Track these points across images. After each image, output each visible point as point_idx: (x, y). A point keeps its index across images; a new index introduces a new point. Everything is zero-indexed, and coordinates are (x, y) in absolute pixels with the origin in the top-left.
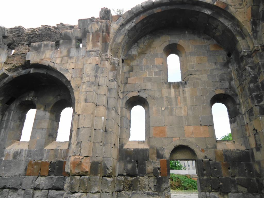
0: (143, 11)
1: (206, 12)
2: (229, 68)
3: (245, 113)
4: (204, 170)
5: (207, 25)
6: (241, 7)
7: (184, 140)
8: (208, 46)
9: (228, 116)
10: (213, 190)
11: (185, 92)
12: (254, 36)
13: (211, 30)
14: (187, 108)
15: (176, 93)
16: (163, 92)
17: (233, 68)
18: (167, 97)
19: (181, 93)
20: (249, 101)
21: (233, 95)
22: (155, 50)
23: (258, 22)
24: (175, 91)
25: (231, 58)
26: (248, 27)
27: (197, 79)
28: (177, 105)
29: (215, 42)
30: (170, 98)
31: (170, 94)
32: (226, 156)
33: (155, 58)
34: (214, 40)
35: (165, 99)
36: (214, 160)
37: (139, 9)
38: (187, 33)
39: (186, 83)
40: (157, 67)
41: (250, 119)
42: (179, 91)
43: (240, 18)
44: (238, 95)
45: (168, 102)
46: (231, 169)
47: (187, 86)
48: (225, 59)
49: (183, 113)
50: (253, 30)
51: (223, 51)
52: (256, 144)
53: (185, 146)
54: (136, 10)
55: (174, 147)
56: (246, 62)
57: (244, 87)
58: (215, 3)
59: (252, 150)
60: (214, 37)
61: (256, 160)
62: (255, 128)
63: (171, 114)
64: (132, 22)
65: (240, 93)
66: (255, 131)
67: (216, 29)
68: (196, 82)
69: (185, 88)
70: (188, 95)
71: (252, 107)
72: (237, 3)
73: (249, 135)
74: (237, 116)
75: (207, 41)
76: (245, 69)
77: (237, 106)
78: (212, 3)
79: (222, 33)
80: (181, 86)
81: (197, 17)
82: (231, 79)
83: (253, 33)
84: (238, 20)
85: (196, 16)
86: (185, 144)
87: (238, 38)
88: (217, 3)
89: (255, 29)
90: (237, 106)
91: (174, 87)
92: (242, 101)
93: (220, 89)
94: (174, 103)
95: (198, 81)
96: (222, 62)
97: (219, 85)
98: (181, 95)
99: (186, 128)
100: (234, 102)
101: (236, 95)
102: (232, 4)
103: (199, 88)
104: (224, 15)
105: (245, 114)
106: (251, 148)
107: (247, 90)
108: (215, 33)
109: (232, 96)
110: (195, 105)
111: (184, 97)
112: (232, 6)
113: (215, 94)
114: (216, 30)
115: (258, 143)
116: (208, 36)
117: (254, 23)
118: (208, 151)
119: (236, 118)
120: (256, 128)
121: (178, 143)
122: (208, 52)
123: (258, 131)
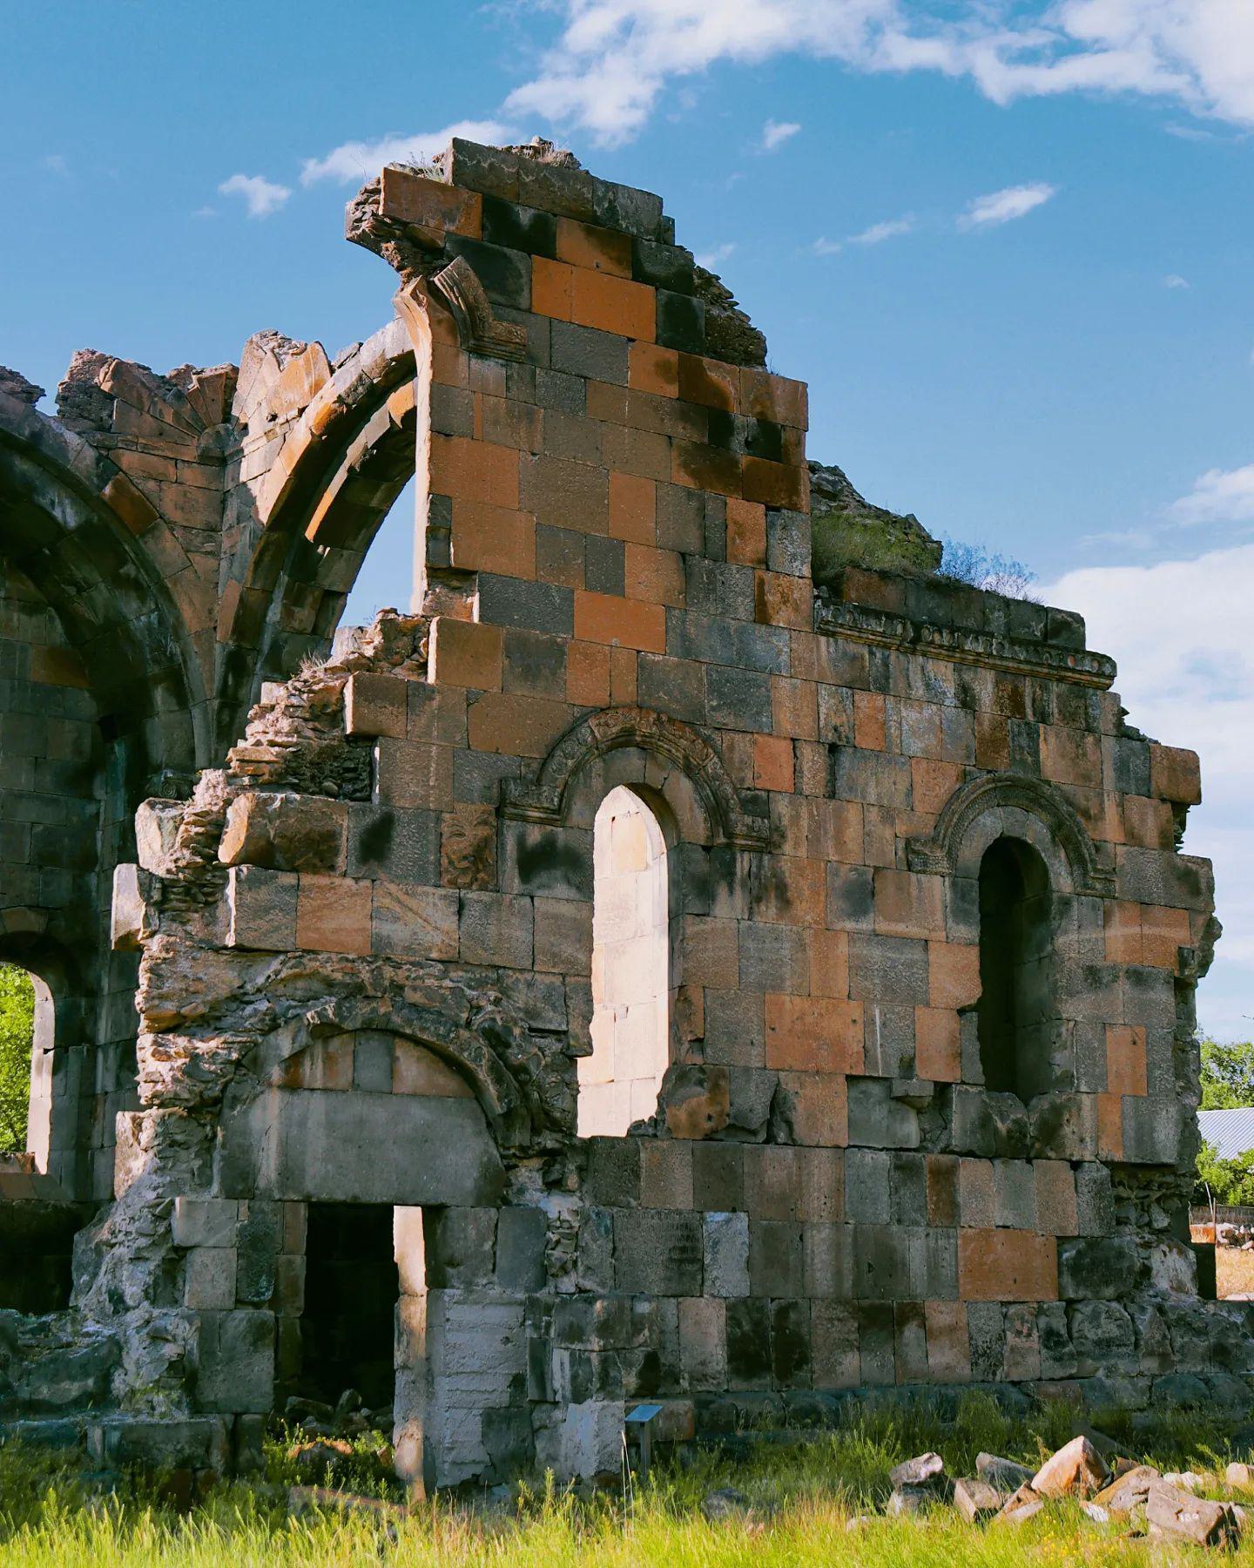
1: (57, 513)
2: (90, 798)
6: (209, 547)
12: (219, 722)
41: (118, 1078)
44: (101, 950)
50: (223, 691)
51: (87, 695)
72: (199, 520)
75: (24, 617)
88: (115, 487)
89: (230, 691)
93: (30, 907)
97: (27, 885)
102: (177, 516)
105: (105, 1047)
112: (172, 530)
116: (30, 587)
122: (12, 689)
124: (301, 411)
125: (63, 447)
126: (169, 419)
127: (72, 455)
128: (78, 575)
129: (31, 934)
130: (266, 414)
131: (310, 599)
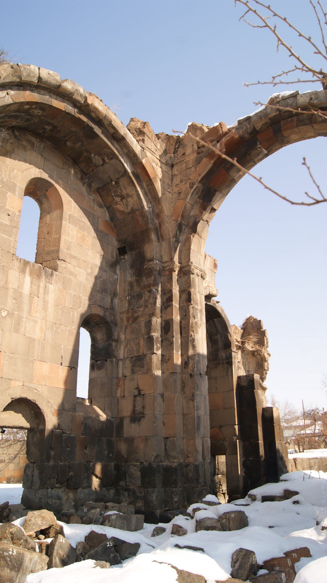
0: (35, 84)
2: (115, 272)
3: (124, 359)
4: (52, 449)
5: (114, 183)
6: (169, 190)
7: (30, 389)
8: (98, 218)
9: (90, 354)
10: (57, 486)
11: (48, 292)
13: (113, 194)
14: (46, 325)
15: (34, 287)
16: (9, 276)
17: (124, 276)
18: (15, 291)
19: (41, 291)
20: (142, 343)
21: (112, 322)
22: (12, 175)
23: (183, 228)
24: (32, 283)
25: (124, 259)
26: (169, 227)
27: (72, 273)
28: (29, 312)
29: (107, 217)
30: (21, 295)
31: (21, 285)
32: (85, 425)
33: (9, 193)
34: (107, 213)
35: (11, 293)
36: (68, 432)
37: (34, 77)
38: (72, 172)
39: (52, 274)
40: (9, 215)
42: (39, 286)
43: (167, 209)
45: (14, 301)
46: (88, 449)
47: (53, 282)
48: (115, 256)
49: (37, 335)
50: (176, 236)
52: (134, 411)
53: (30, 400)
54: (28, 75)
55: (10, 401)
56: (154, 281)
57: (138, 317)
58: (144, 161)
59: (122, 420)
60: (109, 208)
61: (125, 435)
62: (139, 387)
63: (17, 331)
64: (8, 94)
65: (125, 323)
66: (136, 392)
67: (122, 198)
68: (69, 279)
69: (49, 282)
70: (51, 298)
71: (145, 353)
73: (122, 396)
74: (108, 360)
75: (98, 208)
76: (150, 291)
77: (114, 344)
78: (140, 157)
79: (129, 211)
80: (44, 277)
81: (107, 161)
82: (114, 295)
83: (176, 241)
84: (162, 208)
85: (106, 158)
86: (30, 397)
87: (153, 236)
88: (146, 161)
89: (178, 236)
90: (114, 344)
91: (31, 274)
92: (125, 338)
94: (26, 308)
95: (71, 277)
96: (110, 257)
97: (98, 297)
98: (39, 296)
99: (38, 365)
100: (109, 335)
101: (116, 324)
103: (70, 292)
104: (145, 186)
105: (124, 360)
106: (119, 416)
107: (143, 324)
108: (117, 203)
109: (111, 324)
110: (59, 323)
111: (44, 301)
113: (90, 313)
114: (121, 200)
115: (138, 408)
117: (180, 227)
118: (64, 414)
119: (106, 362)
120: (141, 387)
121: (18, 394)
123: (142, 393)
124: (218, 142)
125: (132, 142)
126: (159, 147)
127: (134, 146)
128: (124, 192)
129: (99, 316)
130: (196, 147)
131: (208, 209)
